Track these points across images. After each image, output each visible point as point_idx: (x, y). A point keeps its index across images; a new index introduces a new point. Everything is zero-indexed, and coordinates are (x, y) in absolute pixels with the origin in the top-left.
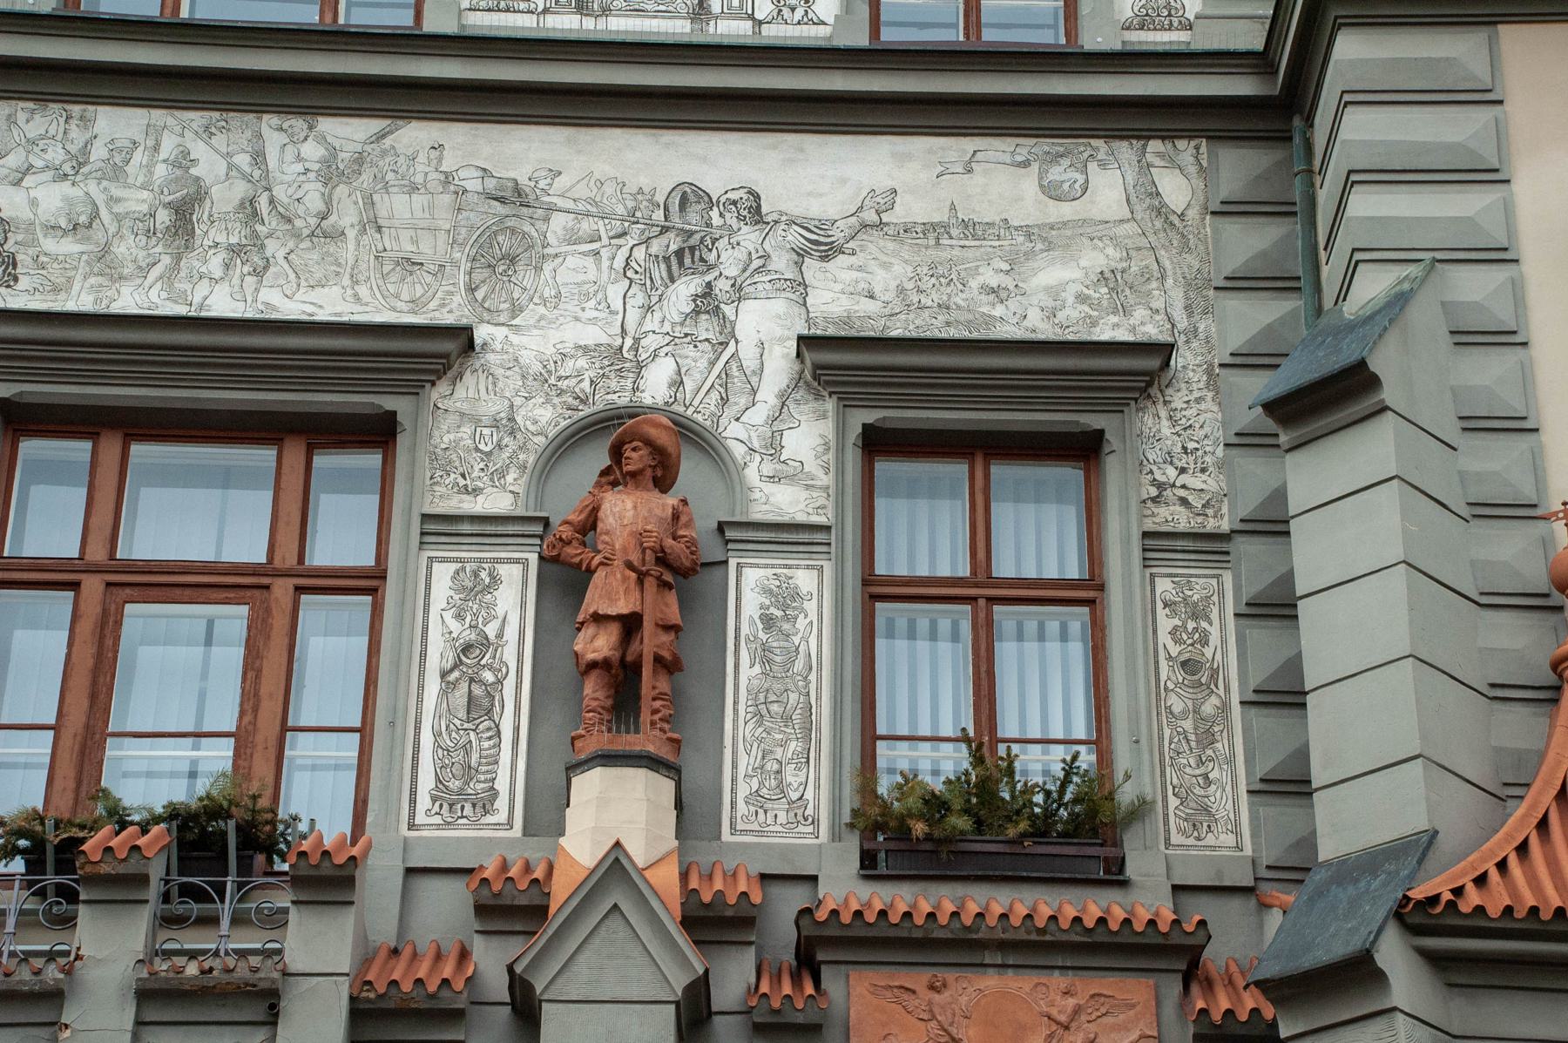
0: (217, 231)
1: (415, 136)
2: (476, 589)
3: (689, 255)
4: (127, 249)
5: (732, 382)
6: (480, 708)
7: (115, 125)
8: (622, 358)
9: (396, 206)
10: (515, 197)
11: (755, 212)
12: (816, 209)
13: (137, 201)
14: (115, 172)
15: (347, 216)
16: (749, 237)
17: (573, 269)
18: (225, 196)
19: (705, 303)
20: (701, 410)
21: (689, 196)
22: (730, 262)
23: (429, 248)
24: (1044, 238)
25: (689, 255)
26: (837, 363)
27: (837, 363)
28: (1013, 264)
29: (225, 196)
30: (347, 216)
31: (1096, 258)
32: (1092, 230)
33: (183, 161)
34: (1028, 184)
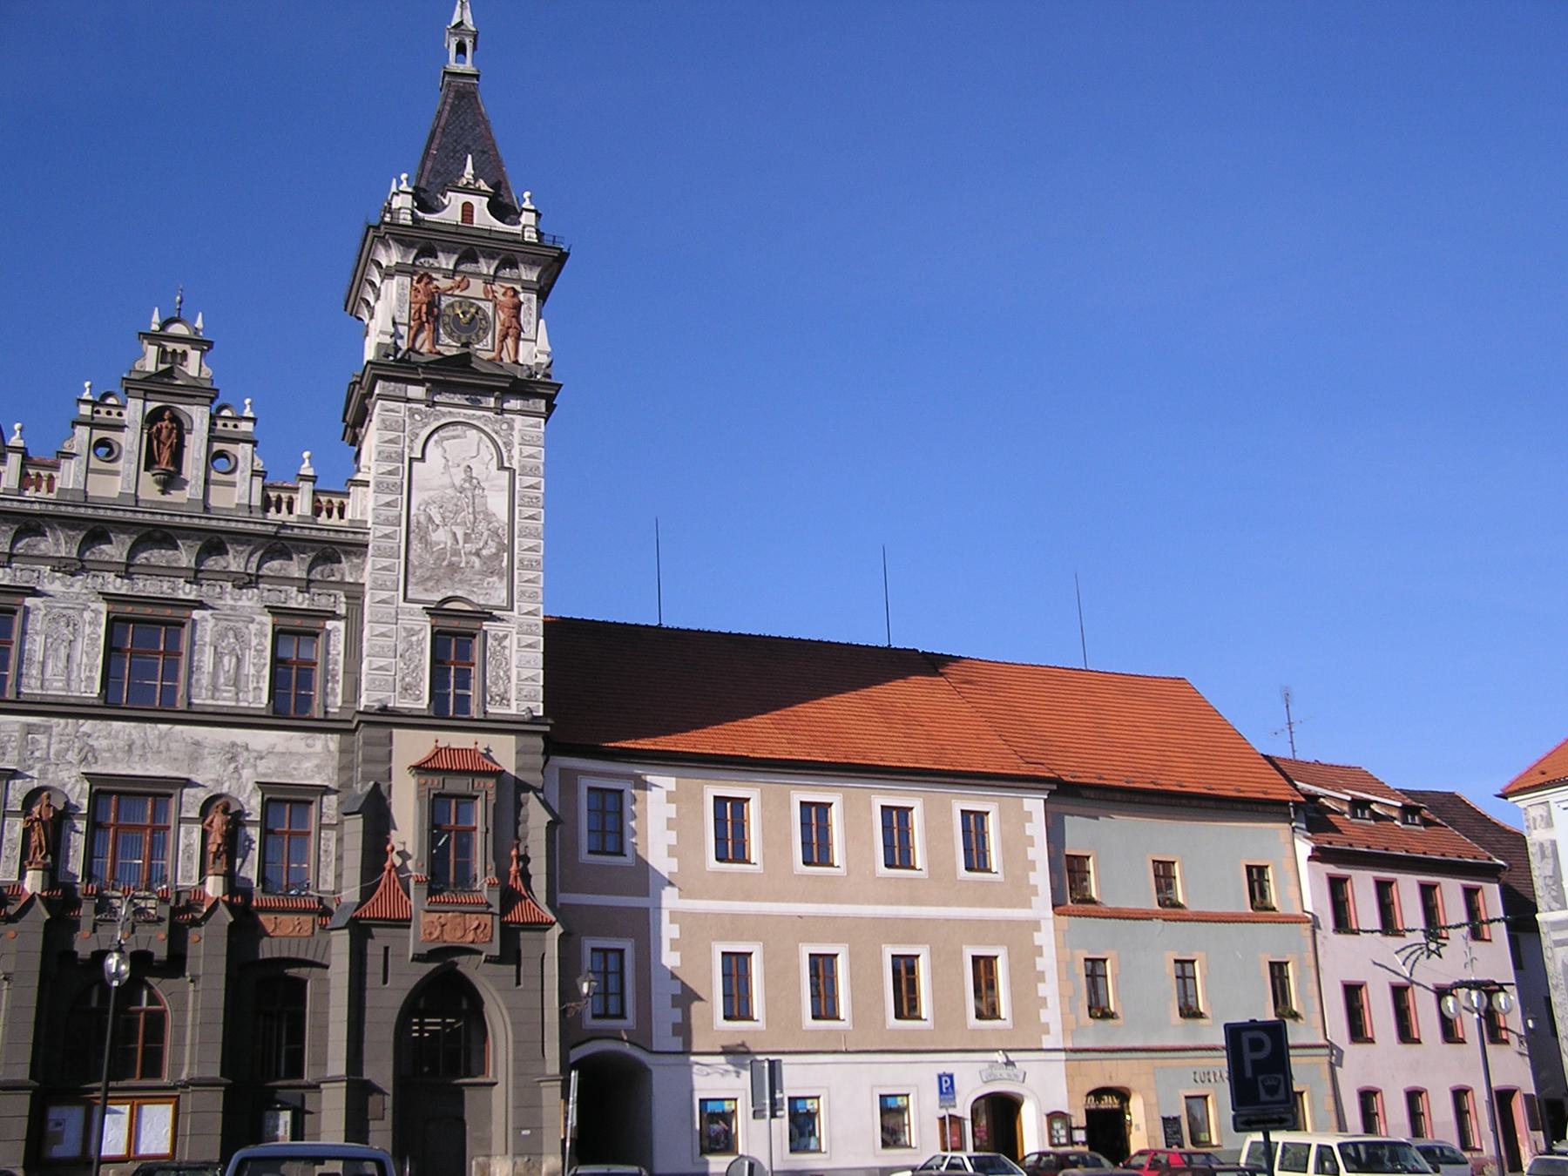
0: (137, 752)
1: (178, 728)
2: (189, 833)
3: (233, 759)
4: (119, 755)
5: (241, 788)
6: (190, 858)
7: (117, 725)
8: (219, 782)
9: (173, 745)
10: (197, 744)
11: (247, 749)
12: (259, 748)
13: (121, 744)
14: (117, 737)
15: (163, 748)
16: (246, 754)
17: (209, 761)
18: (139, 743)
19: (236, 769)
20: (234, 794)
21: (234, 745)
22: (241, 760)
23: (179, 756)
24: (306, 756)
25: (233, 759)
26: (263, 786)
27: (263, 786)
28: (299, 762)
29: (139, 743)
30: (163, 748)
31: (315, 761)
32: (315, 754)
33: (130, 735)
34: (303, 744)
